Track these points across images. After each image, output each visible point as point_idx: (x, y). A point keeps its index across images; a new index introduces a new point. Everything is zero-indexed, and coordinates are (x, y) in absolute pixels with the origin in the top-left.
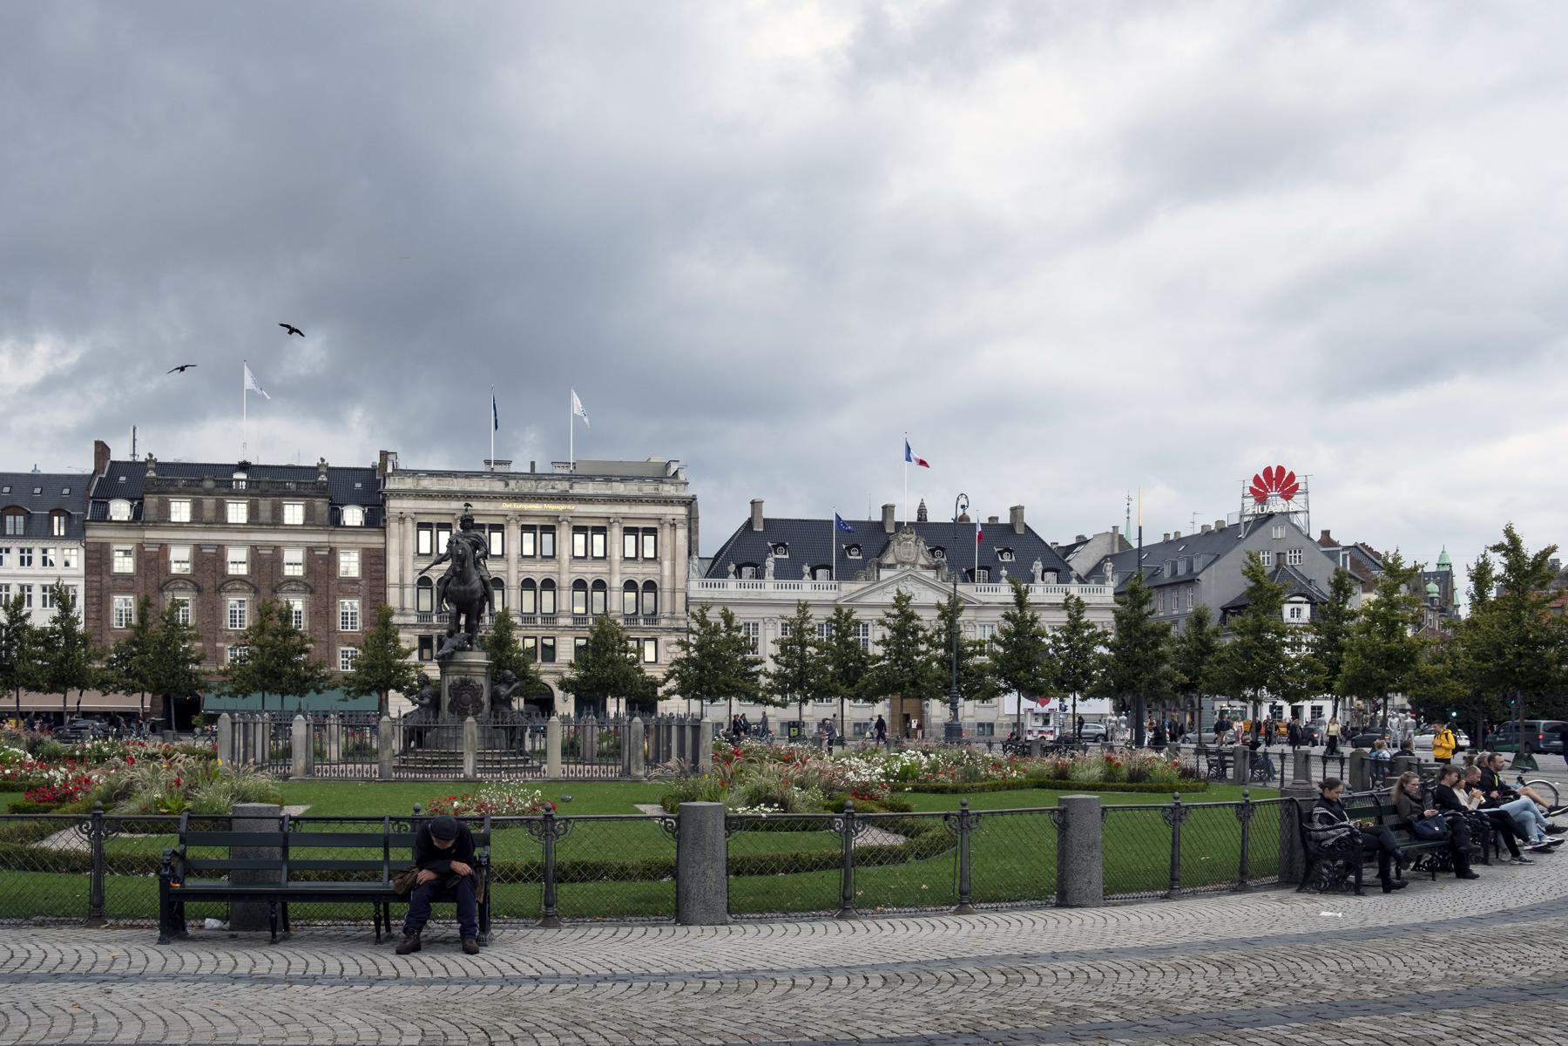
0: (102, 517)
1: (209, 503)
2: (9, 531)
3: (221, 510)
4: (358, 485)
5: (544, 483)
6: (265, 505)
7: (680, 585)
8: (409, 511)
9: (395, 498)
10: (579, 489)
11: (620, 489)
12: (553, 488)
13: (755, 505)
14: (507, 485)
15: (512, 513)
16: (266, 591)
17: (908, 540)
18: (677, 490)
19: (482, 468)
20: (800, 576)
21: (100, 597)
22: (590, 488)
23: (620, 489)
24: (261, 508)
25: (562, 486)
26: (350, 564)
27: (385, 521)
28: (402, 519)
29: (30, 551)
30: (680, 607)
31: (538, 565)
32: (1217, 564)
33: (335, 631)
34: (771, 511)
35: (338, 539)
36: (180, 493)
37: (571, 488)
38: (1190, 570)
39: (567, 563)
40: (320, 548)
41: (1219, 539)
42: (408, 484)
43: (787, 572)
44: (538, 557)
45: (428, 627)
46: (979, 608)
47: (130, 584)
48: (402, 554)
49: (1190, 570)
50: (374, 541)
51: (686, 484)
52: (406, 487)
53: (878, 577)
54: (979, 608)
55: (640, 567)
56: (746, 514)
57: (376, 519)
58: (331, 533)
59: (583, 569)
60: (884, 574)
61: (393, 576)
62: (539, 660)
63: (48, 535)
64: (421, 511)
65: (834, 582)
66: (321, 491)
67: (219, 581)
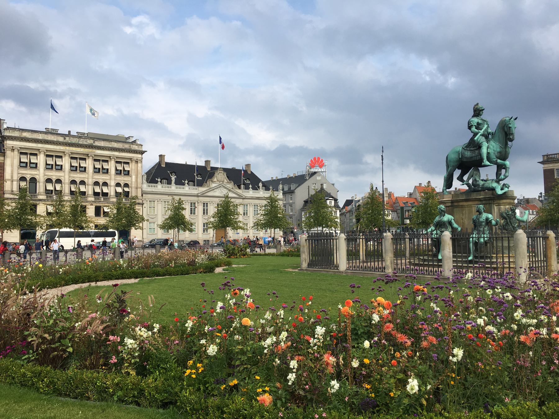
5: (82, 139)
8: (17, 146)
9: (10, 140)
10: (97, 143)
11: (115, 145)
12: (86, 142)
13: (161, 157)
14: (65, 139)
15: (67, 151)
19: (45, 130)
23: (115, 145)
25: (90, 142)
27: (4, 150)
31: (78, 175)
32: (300, 187)
34: (168, 159)
37: (94, 143)
38: (290, 188)
41: (300, 180)
42: (16, 134)
43: (179, 182)
48: (12, 166)
49: (290, 188)
51: (142, 145)
55: (123, 177)
56: (157, 160)
61: (7, 175)
64: (23, 147)
65: (196, 187)
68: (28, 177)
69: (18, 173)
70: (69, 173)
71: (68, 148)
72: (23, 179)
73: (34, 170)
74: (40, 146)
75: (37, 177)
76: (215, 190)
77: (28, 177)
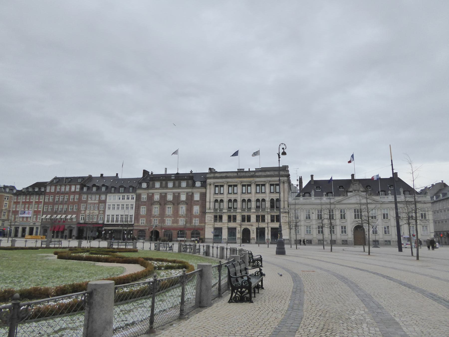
0: (140, 188)
1: (164, 183)
2: (121, 192)
3: (167, 184)
6: (177, 183)
7: (286, 199)
10: (257, 174)
11: (268, 173)
12: (250, 174)
16: (176, 204)
17: (356, 183)
18: (284, 173)
23: (268, 173)
24: (176, 183)
26: (197, 197)
28: (210, 185)
29: (129, 196)
30: (286, 206)
33: (193, 214)
35: (194, 190)
39: (254, 194)
40: (190, 193)
44: (246, 193)
45: (216, 213)
46: (381, 204)
48: (210, 193)
50: (203, 190)
52: (212, 176)
53: (347, 195)
54: (381, 204)
57: (204, 185)
58: (192, 189)
59: (259, 196)
60: (349, 194)
61: (208, 200)
62: (246, 222)
63: (129, 192)
67: (152, 202)
68: (219, 200)
69: (214, 198)
72: (216, 201)
73: (222, 195)
74: (224, 180)
76: (351, 199)
77: (219, 200)
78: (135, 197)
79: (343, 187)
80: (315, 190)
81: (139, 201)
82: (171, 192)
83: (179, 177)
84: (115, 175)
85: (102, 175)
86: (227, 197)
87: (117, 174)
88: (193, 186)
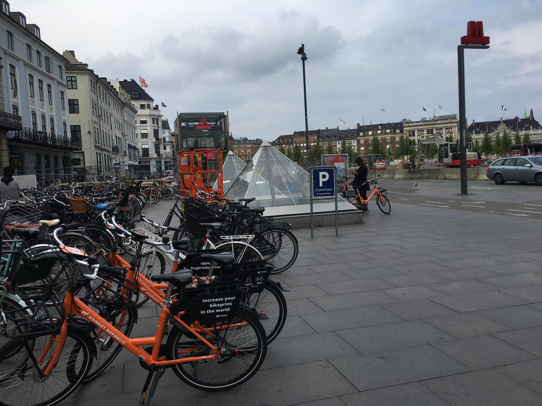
1: (375, 131)
4: (399, 126)
6: (384, 131)
10: (437, 122)
13: (474, 121)
20: (480, 133)
21: (359, 148)
22: (439, 122)
23: (445, 121)
25: (434, 122)
34: (476, 122)
35: (396, 135)
36: (370, 131)
40: (393, 137)
42: (407, 125)
47: (363, 145)
50: (401, 135)
57: (402, 132)
58: (394, 134)
66: (393, 128)
70: (445, 134)
71: (425, 126)
75: (415, 139)
78: (356, 141)
79: (494, 126)
80: (475, 130)
81: (359, 144)
82: (380, 137)
83: (384, 127)
84: (337, 128)
85: (327, 128)
86: (418, 138)
87: (338, 127)
88: (395, 132)
